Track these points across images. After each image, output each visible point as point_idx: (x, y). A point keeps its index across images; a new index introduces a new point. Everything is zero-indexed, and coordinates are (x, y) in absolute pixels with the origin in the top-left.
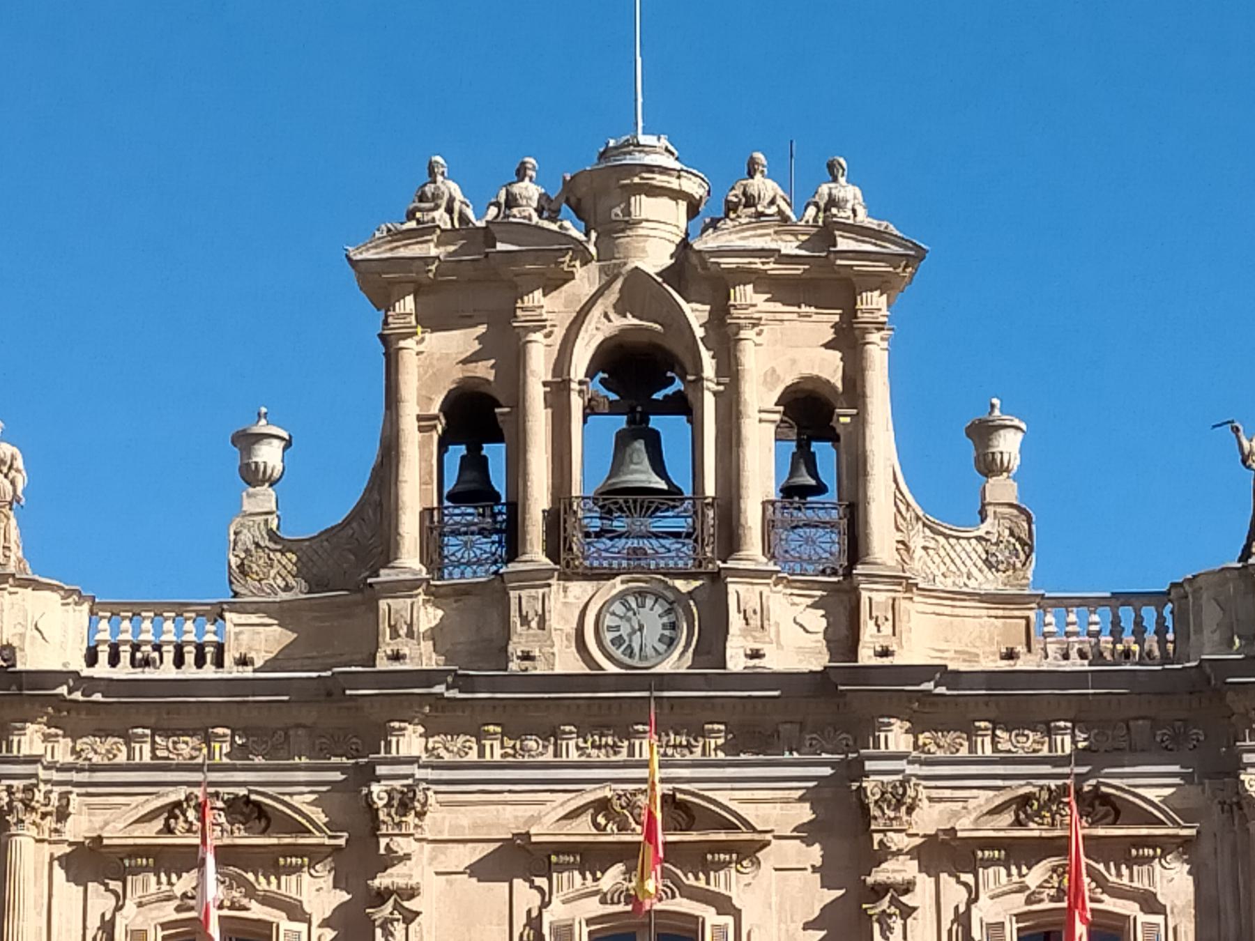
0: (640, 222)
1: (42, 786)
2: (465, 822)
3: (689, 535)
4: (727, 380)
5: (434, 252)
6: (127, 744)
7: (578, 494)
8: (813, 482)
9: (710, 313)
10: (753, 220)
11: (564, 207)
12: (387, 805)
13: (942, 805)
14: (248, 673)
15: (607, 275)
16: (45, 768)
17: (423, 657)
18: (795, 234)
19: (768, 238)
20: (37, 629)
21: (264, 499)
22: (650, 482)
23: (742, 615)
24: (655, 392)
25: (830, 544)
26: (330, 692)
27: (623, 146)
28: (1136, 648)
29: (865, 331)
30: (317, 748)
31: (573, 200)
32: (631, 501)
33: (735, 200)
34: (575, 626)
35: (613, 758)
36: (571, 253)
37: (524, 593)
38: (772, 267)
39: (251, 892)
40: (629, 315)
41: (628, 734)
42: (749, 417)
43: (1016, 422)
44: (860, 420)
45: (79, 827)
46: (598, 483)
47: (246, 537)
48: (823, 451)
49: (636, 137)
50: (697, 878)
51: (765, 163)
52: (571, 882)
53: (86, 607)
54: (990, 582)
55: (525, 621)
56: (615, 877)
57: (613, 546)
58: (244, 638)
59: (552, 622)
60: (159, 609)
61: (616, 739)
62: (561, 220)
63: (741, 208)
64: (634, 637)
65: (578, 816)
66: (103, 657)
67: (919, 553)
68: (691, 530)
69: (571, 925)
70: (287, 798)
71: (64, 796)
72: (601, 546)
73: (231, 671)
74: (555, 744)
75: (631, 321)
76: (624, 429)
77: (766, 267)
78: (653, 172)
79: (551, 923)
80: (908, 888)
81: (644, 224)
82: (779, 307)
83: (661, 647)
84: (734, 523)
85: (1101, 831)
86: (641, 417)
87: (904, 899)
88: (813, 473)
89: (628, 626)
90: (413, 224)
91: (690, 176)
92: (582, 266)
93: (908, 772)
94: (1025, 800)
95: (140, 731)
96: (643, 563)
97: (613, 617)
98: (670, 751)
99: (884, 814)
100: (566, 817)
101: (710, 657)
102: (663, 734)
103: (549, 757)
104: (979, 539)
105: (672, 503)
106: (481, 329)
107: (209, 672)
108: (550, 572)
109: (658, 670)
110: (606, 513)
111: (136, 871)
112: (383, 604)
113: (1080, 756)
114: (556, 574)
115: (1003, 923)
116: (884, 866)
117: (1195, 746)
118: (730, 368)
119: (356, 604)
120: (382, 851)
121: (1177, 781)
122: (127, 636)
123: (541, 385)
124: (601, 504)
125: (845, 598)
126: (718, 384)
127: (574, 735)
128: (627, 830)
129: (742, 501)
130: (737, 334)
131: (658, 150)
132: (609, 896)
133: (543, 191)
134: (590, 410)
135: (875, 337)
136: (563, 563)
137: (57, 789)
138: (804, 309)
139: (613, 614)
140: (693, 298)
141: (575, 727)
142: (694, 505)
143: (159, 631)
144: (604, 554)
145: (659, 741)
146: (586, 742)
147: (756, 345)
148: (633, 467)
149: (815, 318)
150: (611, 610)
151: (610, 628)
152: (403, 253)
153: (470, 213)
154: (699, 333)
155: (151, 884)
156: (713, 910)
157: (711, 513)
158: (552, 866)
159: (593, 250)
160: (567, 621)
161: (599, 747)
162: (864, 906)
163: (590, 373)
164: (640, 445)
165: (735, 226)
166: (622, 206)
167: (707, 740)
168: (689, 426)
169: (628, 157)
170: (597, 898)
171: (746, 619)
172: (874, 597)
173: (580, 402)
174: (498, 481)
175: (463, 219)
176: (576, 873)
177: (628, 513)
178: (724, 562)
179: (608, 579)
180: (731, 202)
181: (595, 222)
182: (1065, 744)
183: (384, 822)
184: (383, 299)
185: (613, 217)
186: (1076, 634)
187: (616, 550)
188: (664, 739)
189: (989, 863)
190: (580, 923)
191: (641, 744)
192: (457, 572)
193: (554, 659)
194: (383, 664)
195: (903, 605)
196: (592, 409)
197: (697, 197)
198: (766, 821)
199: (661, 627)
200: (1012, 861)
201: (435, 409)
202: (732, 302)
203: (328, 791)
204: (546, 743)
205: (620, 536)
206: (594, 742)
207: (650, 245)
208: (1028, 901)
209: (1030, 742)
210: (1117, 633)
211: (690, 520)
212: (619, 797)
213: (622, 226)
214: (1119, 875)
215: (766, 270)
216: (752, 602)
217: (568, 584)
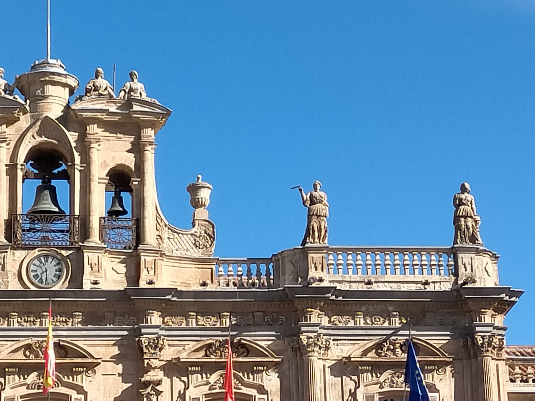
0: (49, 96)
3: (67, 231)
4: (85, 165)
7: (20, 213)
8: (121, 209)
9: (78, 136)
10: (97, 97)
11: (16, 89)
13: (174, 347)
15: (34, 119)
18: (115, 103)
19: (104, 105)
22: (51, 208)
23: (90, 266)
24: (53, 170)
25: (128, 236)
27: (42, 64)
28: (257, 281)
29: (145, 145)
31: (20, 86)
32: (43, 216)
33: (90, 88)
34: (17, 269)
35: (33, 327)
36: (18, 109)
38: (105, 117)
40: (43, 137)
41: (40, 316)
42: (94, 181)
43: (208, 185)
44: (142, 183)
48: (125, 195)
49: (47, 60)
50: (69, 379)
51: (103, 72)
52: (14, 380)
54: (197, 254)
56: (33, 378)
57: (34, 236)
59: (7, 267)
61: (35, 319)
62: (14, 95)
63: (92, 91)
64: (43, 275)
65: (17, 352)
67: (166, 240)
68: (69, 229)
69: (14, 398)
72: (30, 236)
74: (8, 320)
75: (44, 139)
76: (41, 186)
77: (103, 117)
79: (5, 398)
80: (159, 383)
81: (50, 97)
82: (108, 134)
83: (55, 279)
84: (87, 226)
85: (241, 359)
86: (48, 180)
87: (157, 388)
88: (122, 206)
89: (41, 270)
91: (70, 77)
92: (23, 115)
93: (160, 334)
94: (210, 346)
96: (48, 243)
97: (34, 266)
98: (58, 324)
99: (149, 351)
100: (12, 352)
101: (75, 284)
102: (55, 316)
104: (192, 235)
105: (60, 217)
108: (7, 247)
110: (32, 221)
113: (233, 327)
114: (10, 247)
115: (199, 398)
116: (149, 373)
117: (281, 324)
118: (86, 160)
121: (274, 338)
123: (5, 166)
124: (30, 217)
125: (134, 259)
126: (81, 167)
127: (17, 317)
128: (38, 358)
129: (91, 217)
130: (90, 145)
131: (57, 66)
132: (30, 386)
133: (6, 82)
134: (25, 177)
135: (149, 148)
136: (13, 243)
138: (119, 135)
139: (34, 265)
140: (71, 130)
141: (17, 313)
142: (70, 218)
144: (31, 239)
145: (53, 319)
146: (21, 319)
147: (98, 150)
148: (44, 202)
149: (123, 139)
150: (33, 263)
151: (32, 271)
154: (74, 145)
156: (75, 392)
157: (77, 222)
158: (6, 373)
159: (28, 108)
160: (14, 267)
161: (27, 322)
162: (140, 391)
163: (26, 161)
164: (47, 192)
165: (89, 99)
166: (41, 89)
167: (74, 319)
168: (69, 185)
169: (44, 68)
170: (25, 387)
171: (91, 267)
172: (146, 259)
173: (22, 173)
176: (16, 376)
177: (42, 222)
178: (83, 243)
179: (32, 250)
180: (88, 89)
181: (29, 96)
182: (227, 323)
185: (37, 94)
186: (232, 275)
187: (36, 237)
188: (56, 319)
189: (194, 372)
190: (18, 397)
191: (45, 321)
193: (8, 284)
195: (159, 262)
196: (27, 176)
197: (73, 86)
198: (98, 355)
199: (55, 270)
200: (203, 372)
202: (88, 132)
204: (4, 320)
205: (38, 231)
206: (25, 319)
207: (53, 106)
208: (210, 389)
209: (211, 321)
210: (249, 275)
211: (68, 225)
212: (36, 343)
213: (40, 98)
214: (249, 378)
215: (103, 118)
216: (94, 261)
217: (15, 251)
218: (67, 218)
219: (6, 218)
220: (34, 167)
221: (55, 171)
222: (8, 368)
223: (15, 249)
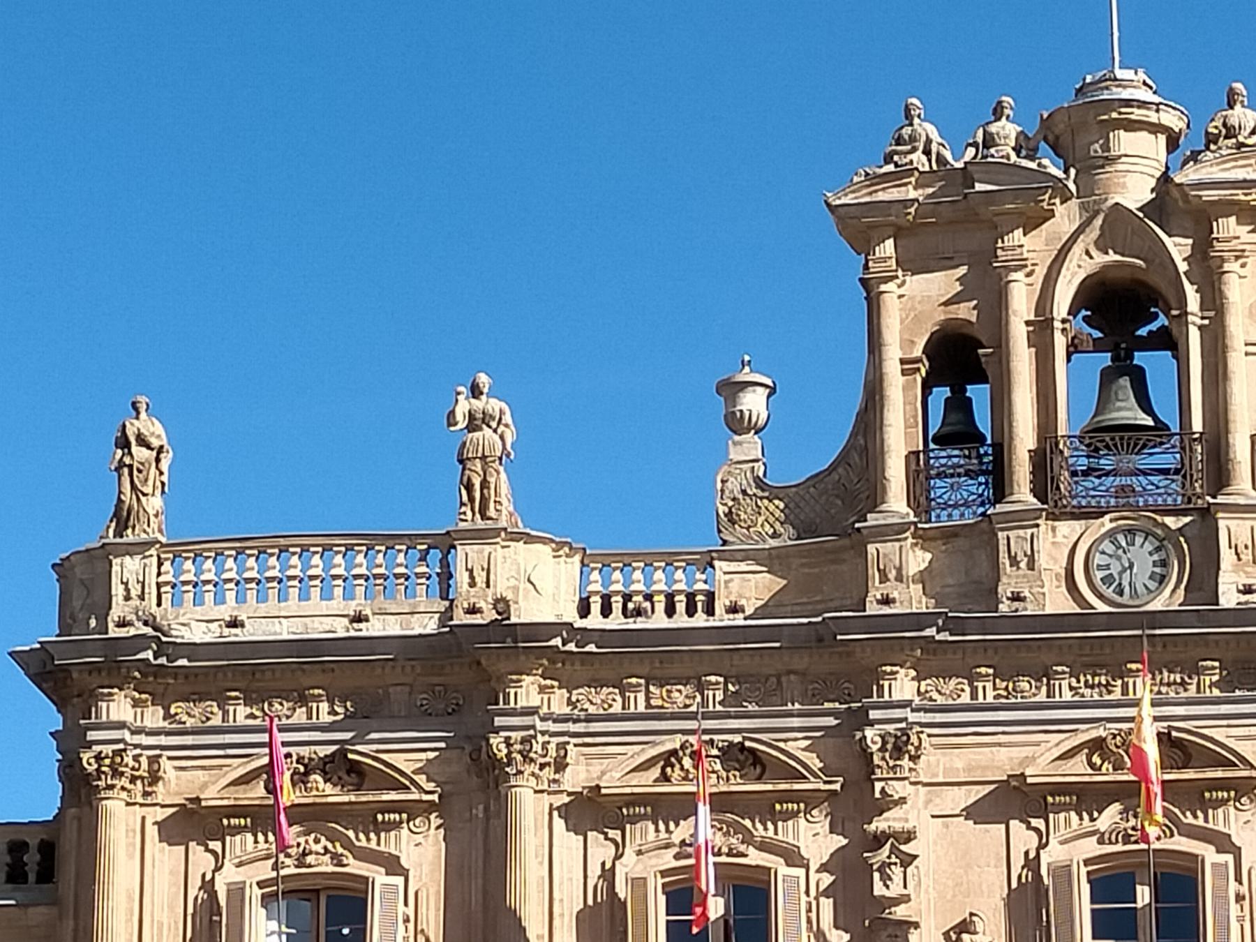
0: (1120, 157)
1: (540, 738)
2: (959, 764)
3: (1177, 472)
4: (1212, 314)
5: (912, 194)
6: (622, 695)
7: (1064, 433)
9: (1193, 246)
10: (1234, 151)
11: (1043, 144)
12: (883, 749)
14: (739, 620)
15: (1087, 211)
16: (543, 719)
17: (912, 600)
19: (1250, 169)
20: (529, 580)
21: (749, 447)
22: (1136, 419)
23: (1233, 550)
24: (1138, 329)
26: (821, 638)
27: (1100, 81)
30: (810, 693)
31: (1051, 137)
32: (1117, 438)
33: (1216, 131)
34: (1064, 565)
35: (1107, 697)
36: (1050, 191)
37: (1012, 534)
39: (748, 839)
40: (1111, 252)
41: (1121, 673)
42: (1235, 350)
45: (577, 777)
46: (1085, 421)
47: (734, 485)
49: (1112, 72)
50: (1195, 817)
51: (1245, 93)
52: (1068, 822)
53: (577, 558)
55: (1014, 562)
56: (1112, 817)
57: (1101, 484)
58: (734, 586)
59: (1041, 561)
60: (649, 560)
61: (1110, 679)
62: (1040, 158)
63: (1221, 139)
64: (1124, 575)
65: (1072, 757)
66: (596, 607)
68: (1179, 466)
69: (1069, 866)
70: (781, 745)
71: (562, 746)
72: (1090, 485)
73: (722, 619)
74: (1048, 684)
75: (1113, 257)
76: (1109, 366)
77: (1249, 198)
78: (1132, 106)
79: (1049, 864)
81: (1124, 159)
83: (1152, 585)
84: (1223, 460)
86: (1126, 353)
89: (1118, 563)
90: (890, 168)
91: (1170, 109)
92: (1062, 203)
95: (634, 680)
96: (1131, 500)
97: (1103, 556)
98: (1164, 689)
101: (1202, 593)
102: (1157, 672)
103: (1042, 697)
105: (1159, 440)
106: (963, 270)
107: (700, 620)
108: (1039, 513)
109: (1149, 608)
110: (1093, 451)
111: (634, 820)
112: (871, 548)
114: (1044, 514)
118: (1214, 302)
119: (843, 549)
120: (877, 795)
122: (618, 587)
123: (1023, 325)
124: (1087, 441)
126: (1203, 318)
127: (1067, 676)
128: (1122, 769)
129: (1230, 436)
130: (1221, 267)
131: (1135, 84)
132: (1107, 836)
133: (1019, 129)
134: (1073, 348)
136: (1052, 503)
137: (555, 740)
139: (1103, 553)
140: (1175, 233)
141: (1067, 667)
142: (1182, 441)
143: (649, 581)
144: (1092, 493)
145: (1153, 678)
146: (1079, 681)
147: (1240, 277)
148: (1119, 404)
150: (1100, 549)
151: (1099, 567)
152: (881, 196)
153: (948, 155)
154: (1183, 267)
155: (647, 832)
156: (1212, 848)
157: (1199, 449)
158: (1049, 807)
159: (1073, 187)
160: (1055, 560)
161: (1092, 687)
163: (1073, 311)
164: (1125, 382)
165: (1216, 158)
166: (1101, 142)
167: (1202, 677)
168: (1175, 361)
169: (1105, 92)
170: (1095, 838)
171: (1237, 554)
173: (1064, 339)
174: (983, 422)
175: (941, 160)
176: (1073, 814)
177: (1115, 451)
178: (1214, 497)
179: (1097, 518)
180: (1212, 134)
181: (1074, 158)
183: (879, 767)
184: (863, 242)
185: (1092, 154)
187: (1103, 488)
188: (1158, 678)
191: (1134, 683)
192: (956, 513)
193: (1044, 600)
194: (872, 609)
196: (1076, 347)
197: (1177, 130)
199: (1151, 564)
201: (918, 352)
202: (1214, 235)
203: (822, 736)
204: (1038, 684)
205: (1107, 474)
206: (1086, 681)
207: (1130, 180)
211: (1178, 456)
212: (1114, 737)
213: (1101, 162)
215: (1249, 201)
217: (1056, 523)
218: (1175, 440)
219: (1032, 448)
220: (1094, 324)
221: (1143, 332)
222: (1053, 796)
223: (1055, 518)
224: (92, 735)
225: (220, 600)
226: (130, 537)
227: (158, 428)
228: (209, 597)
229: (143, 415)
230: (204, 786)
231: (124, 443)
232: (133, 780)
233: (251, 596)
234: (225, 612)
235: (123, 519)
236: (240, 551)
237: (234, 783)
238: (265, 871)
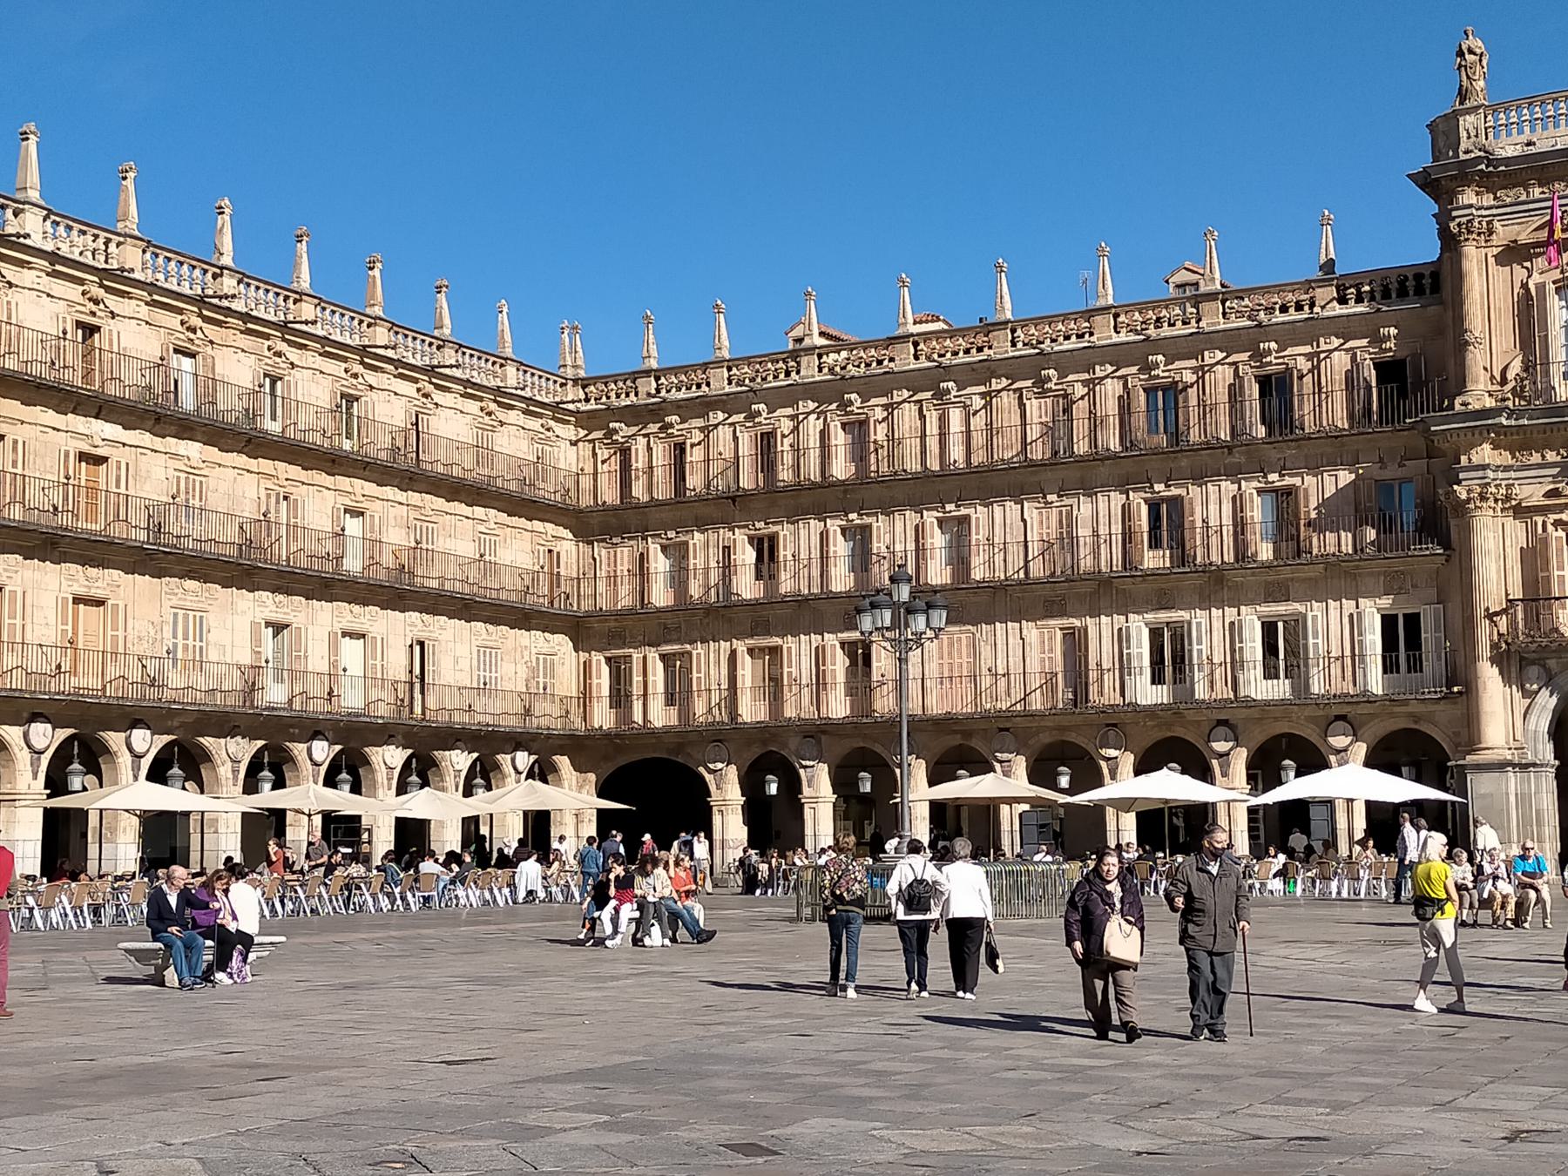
224: (1455, 213)
225: (1520, 132)
226: (1468, 104)
227: (1480, 43)
228: (1515, 131)
229: (1471, 37)
230: (1519, 233)
231: (1461, 54)
232: (1479, 234)
233: (1539, 128)
234: (1524, 138)
235: (1463, 95)
236: (1530, 104)
237: (1536, 230)
238: (1557, 275)
